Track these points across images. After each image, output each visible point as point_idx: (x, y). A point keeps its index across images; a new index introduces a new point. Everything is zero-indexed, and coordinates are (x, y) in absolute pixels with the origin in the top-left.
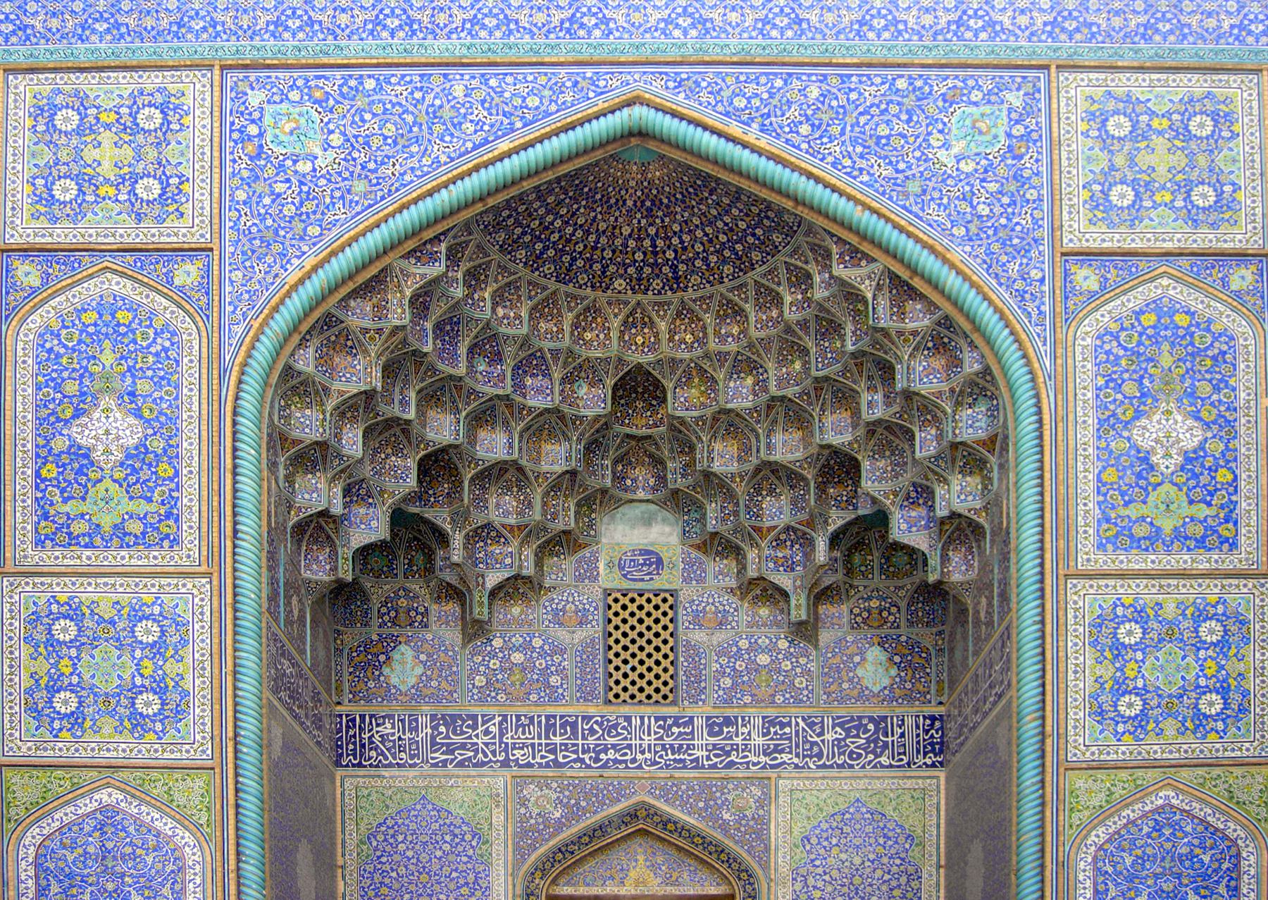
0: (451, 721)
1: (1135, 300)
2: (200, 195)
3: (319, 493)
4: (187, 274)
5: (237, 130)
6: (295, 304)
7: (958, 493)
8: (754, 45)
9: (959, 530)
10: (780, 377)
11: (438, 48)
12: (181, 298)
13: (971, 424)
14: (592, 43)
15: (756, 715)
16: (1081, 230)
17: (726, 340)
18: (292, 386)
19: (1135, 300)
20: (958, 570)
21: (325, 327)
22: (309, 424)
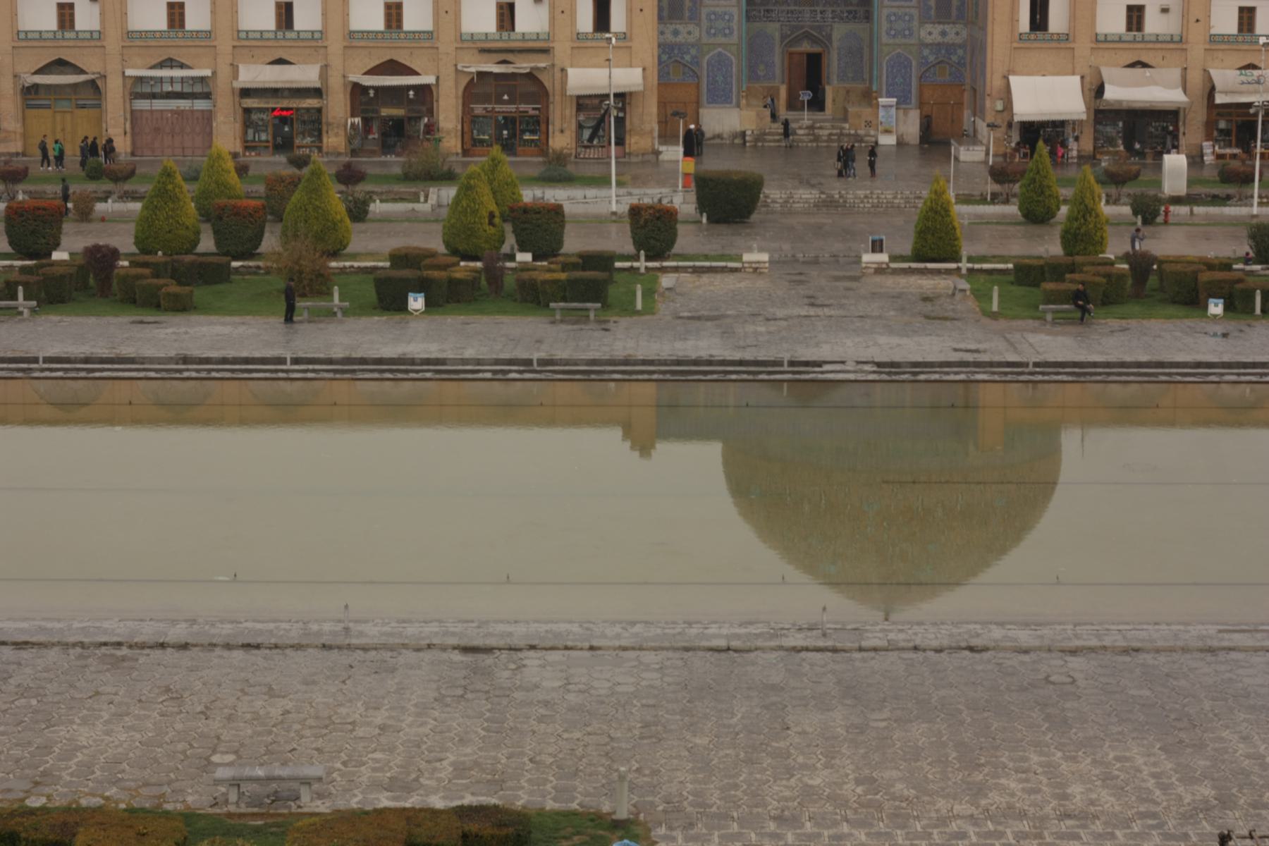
0: (768, 11)
15: (830, 9)
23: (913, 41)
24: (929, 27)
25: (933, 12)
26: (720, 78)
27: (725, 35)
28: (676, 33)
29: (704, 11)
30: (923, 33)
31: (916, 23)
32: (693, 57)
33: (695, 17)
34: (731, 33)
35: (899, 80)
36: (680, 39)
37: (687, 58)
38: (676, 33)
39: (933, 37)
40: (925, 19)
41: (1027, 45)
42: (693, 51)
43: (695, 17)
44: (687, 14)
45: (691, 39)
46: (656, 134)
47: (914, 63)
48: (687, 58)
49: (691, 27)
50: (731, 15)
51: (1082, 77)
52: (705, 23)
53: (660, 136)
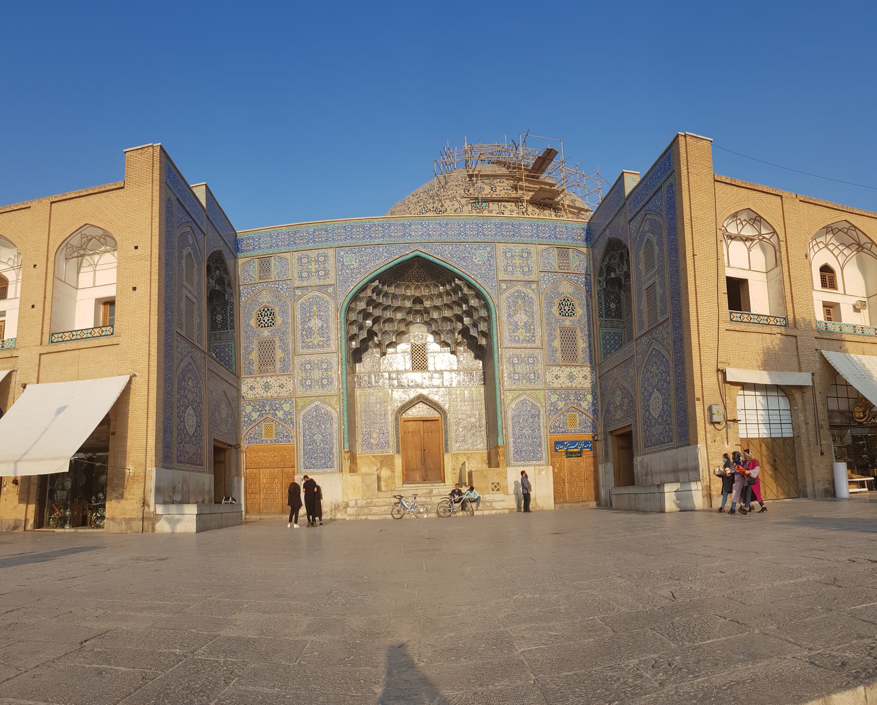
1: (513, 290)
2: (332, 274)
3: (354, 330)
4: (330, 290)
5: (338, 260)
6: (351, 295)
7: (483, 327)
8: (439, 239)
9: (484, 334)
10: (446, 300)
11: (376, 241)
12: (329, 295)
13: (483, 313)
14: (408, 239)
16: (502, 276)
17: (434, 291)
18: (349, 310)
19: (513, 290)
20: (483, 341)
21: (355, 298)
22: (353, 316)
23: (540, 387)
24: (556, 370)
25: (559, 355)
26: (318, 438)
27: (323, 386)
28: (267, 387)
29: (298, 360)
30: (549, 378)
31: (540, 367)
32: (287, 414)
33: (286, 370)
34: (330, 383)
35: (527, 432)
36: (272, 393)
37: (280, 414)
38: (267, 387)
39: (560, 381)
40: (552, 363)
41: (742, 327)
42: (286, 407)
43: (286, 370)
44: (278, 366)
45: (284, 393)
46: (151, 484)
47: (542, 412)
48: (280, 414)
49: (283, 380)
50: (329, 363)
51: (813, 374)
52: (299, 375)
53: (158, 490)
